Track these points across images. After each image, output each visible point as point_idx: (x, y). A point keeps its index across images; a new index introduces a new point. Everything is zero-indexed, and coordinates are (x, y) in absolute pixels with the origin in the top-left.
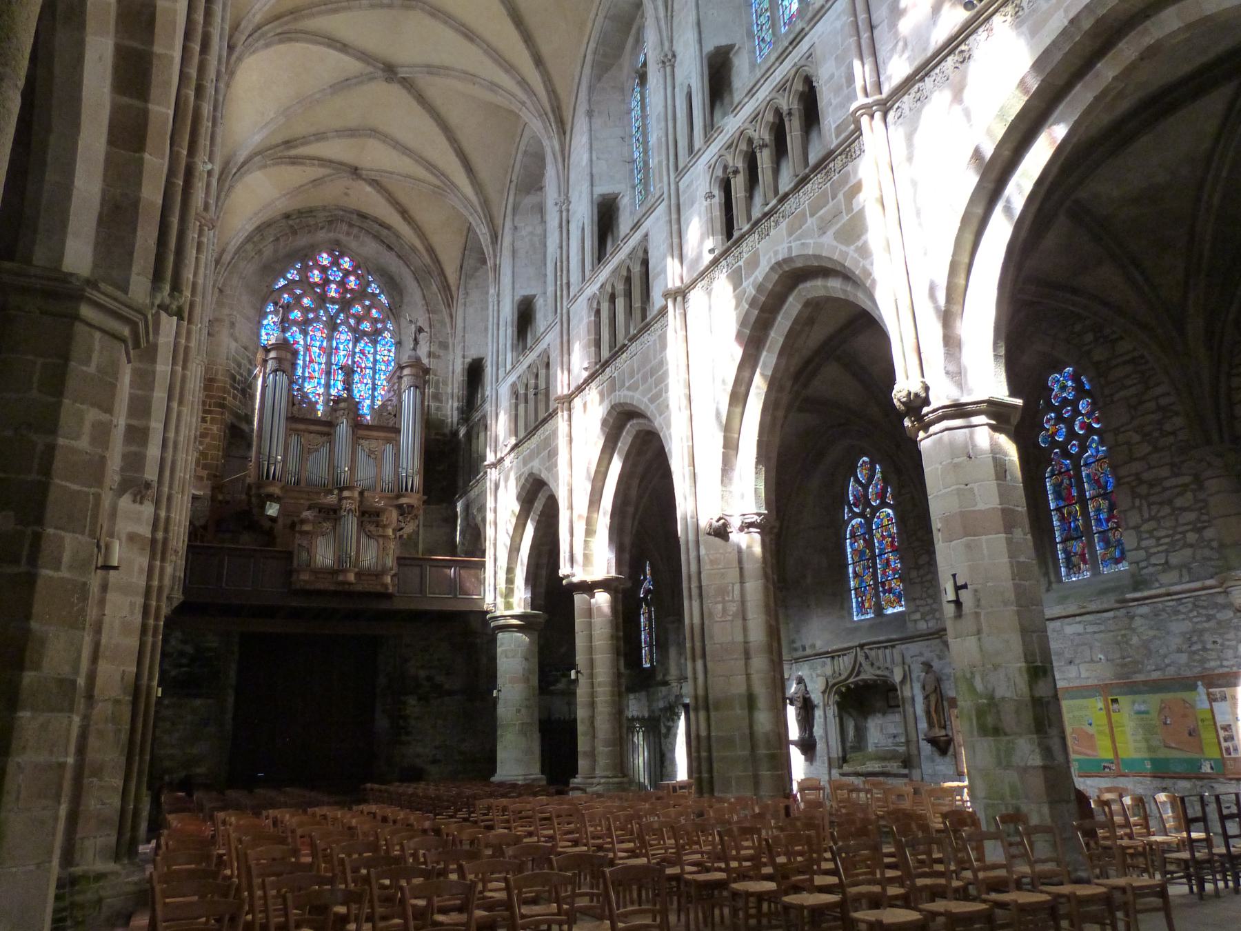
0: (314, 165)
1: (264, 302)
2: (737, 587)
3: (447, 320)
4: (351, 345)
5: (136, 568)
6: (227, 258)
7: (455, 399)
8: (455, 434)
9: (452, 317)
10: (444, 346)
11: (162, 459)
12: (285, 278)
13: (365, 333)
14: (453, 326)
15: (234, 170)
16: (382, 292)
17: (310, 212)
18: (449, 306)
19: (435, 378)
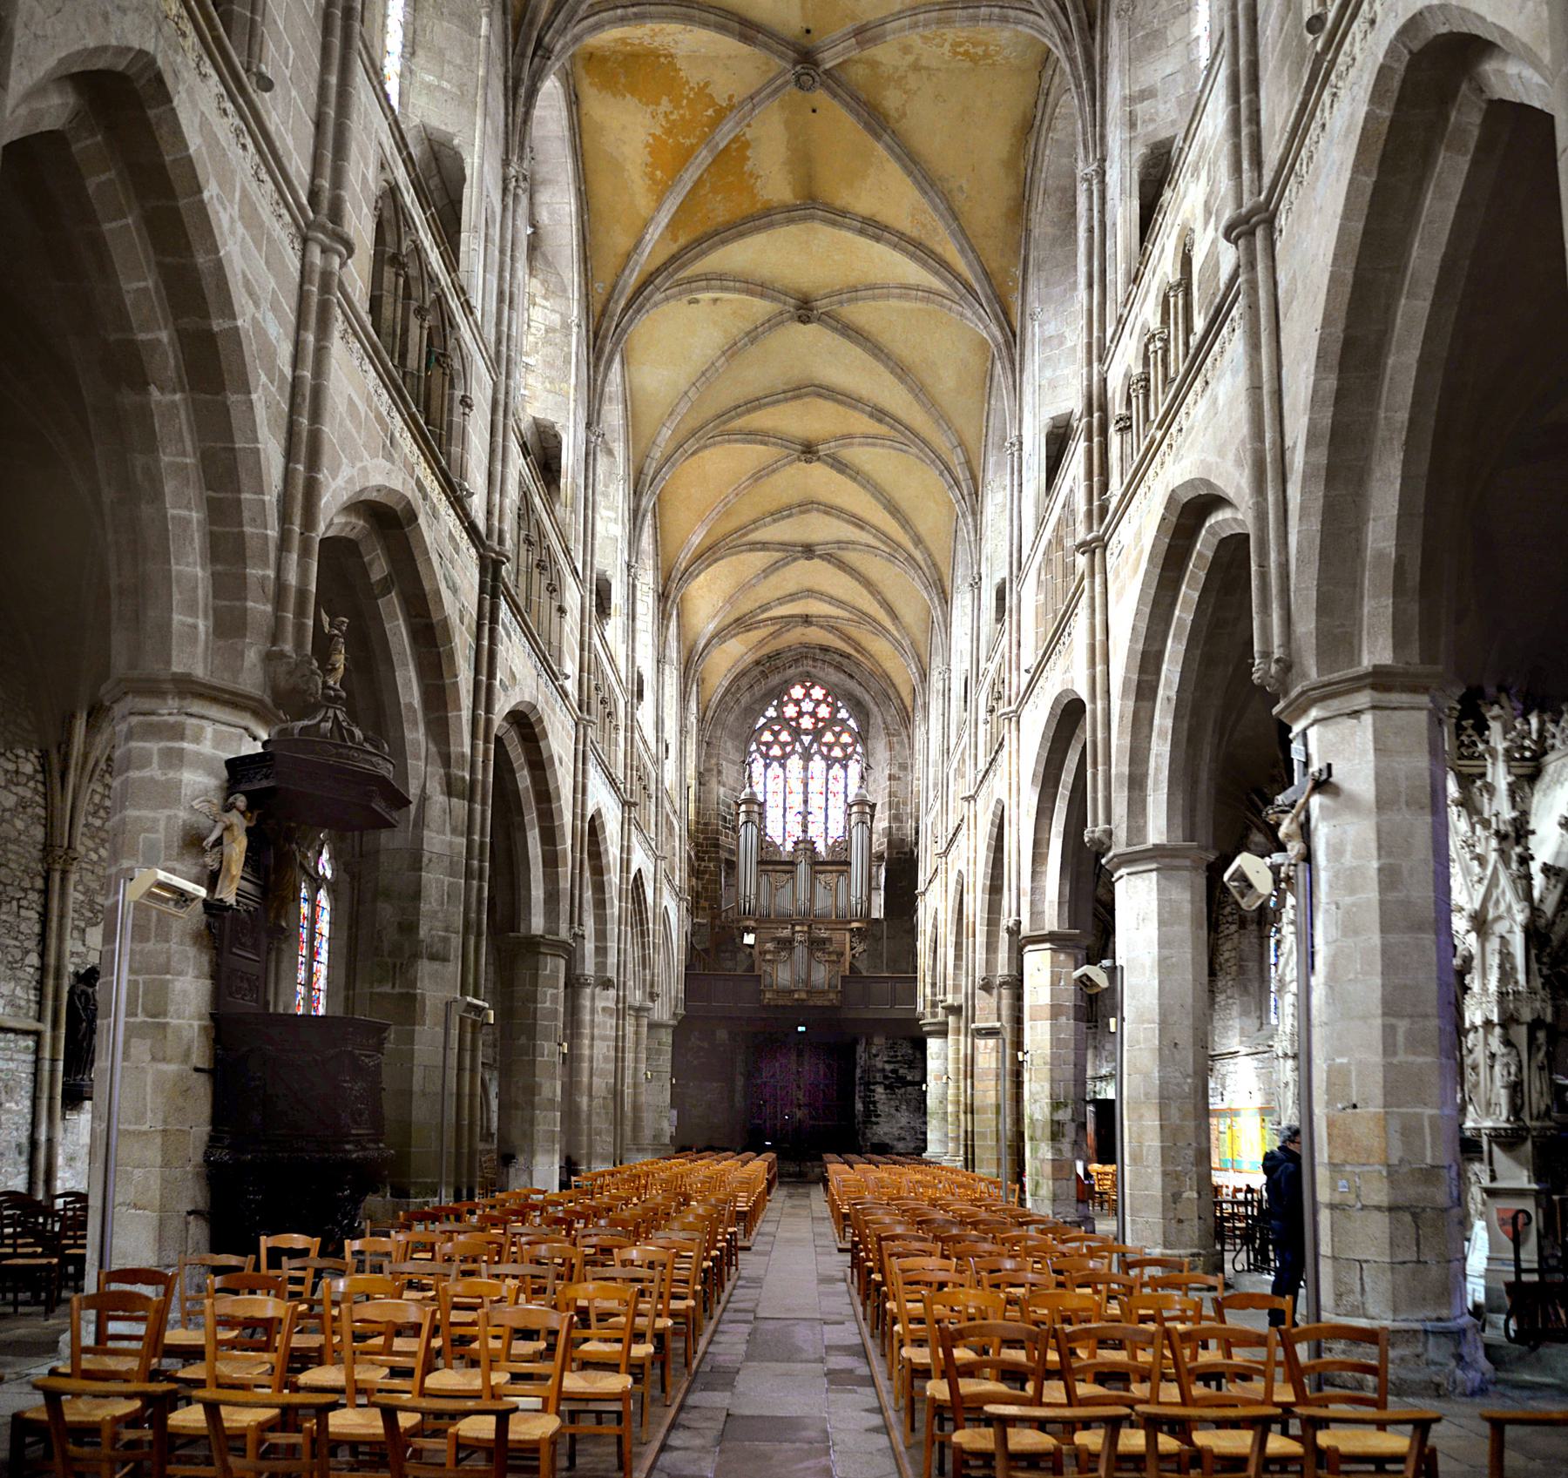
1: (747, 743)
6: (710, 714)
13: (836, 760)
14: (912, 747)
17: (778, 654)
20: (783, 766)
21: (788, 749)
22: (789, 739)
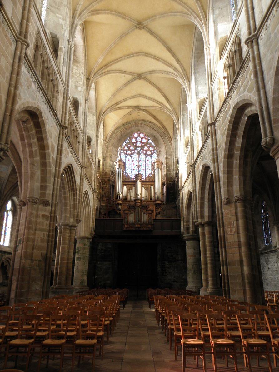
0: (126, 108)
2: (235, 222)
3: (171, 147)
4: (145, 159)
5: (45, 224)
6: (108, 139)
7: (175, 171)
8: (174, 181)
9: (172, 146)
10: (170, 155)
11: (53, 194)
12: (125, 142)
13: (148, 155)
14: (173, 149)
15: (102, 114)
16: (153, 142)
18: (171, 142)
19: (168, 165)
20: (131, 157)
21: (133, 152)
22: (134, 149)
